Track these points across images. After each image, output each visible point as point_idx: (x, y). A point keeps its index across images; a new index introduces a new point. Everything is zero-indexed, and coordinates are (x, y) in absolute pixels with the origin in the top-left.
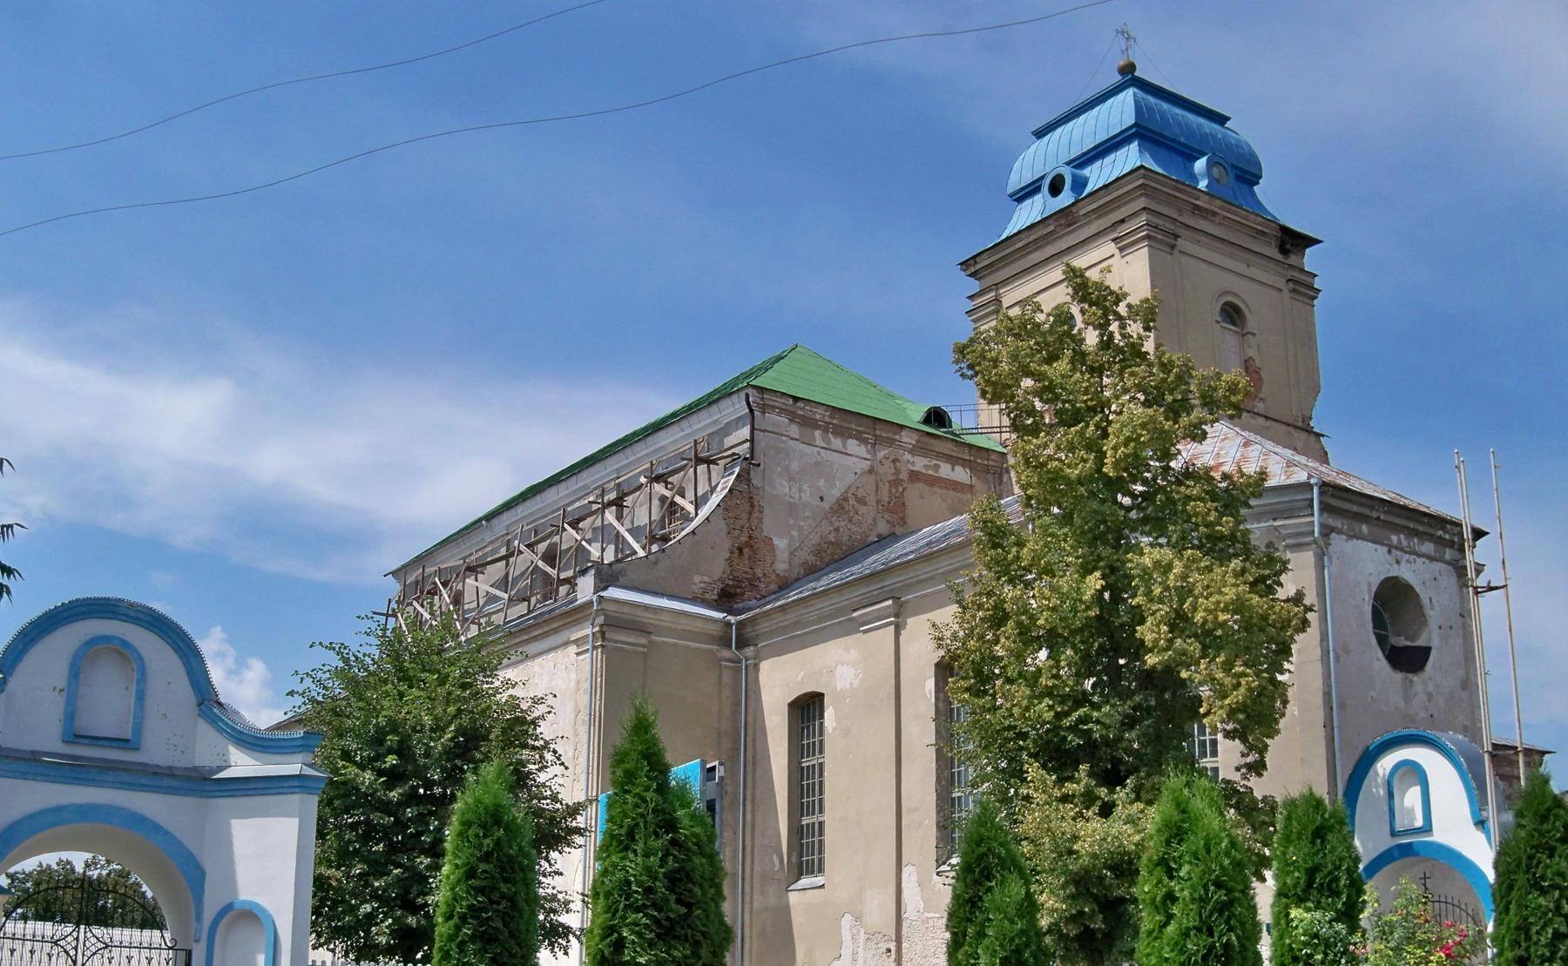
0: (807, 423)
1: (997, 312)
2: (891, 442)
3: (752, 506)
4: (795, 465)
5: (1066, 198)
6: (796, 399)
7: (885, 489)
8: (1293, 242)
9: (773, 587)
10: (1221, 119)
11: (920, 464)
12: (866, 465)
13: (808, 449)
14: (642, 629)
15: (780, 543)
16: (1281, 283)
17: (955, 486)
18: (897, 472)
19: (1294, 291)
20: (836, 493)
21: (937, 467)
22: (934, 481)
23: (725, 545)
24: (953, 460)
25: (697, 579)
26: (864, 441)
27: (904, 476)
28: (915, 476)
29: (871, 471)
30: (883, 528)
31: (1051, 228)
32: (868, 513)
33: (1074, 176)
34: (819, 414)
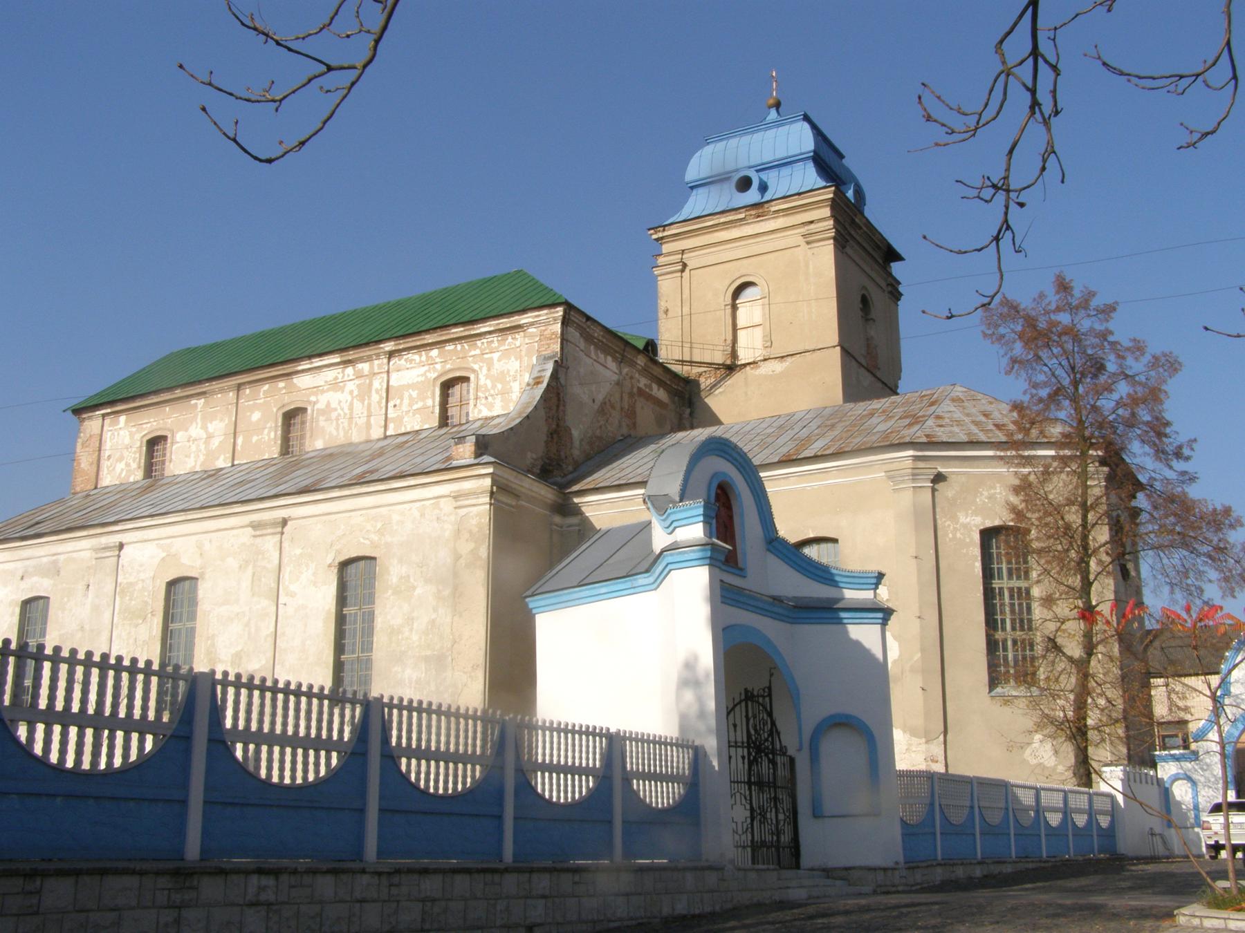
0: (588, 338)
1: (682, 271)
2: (633, 364)
3: (559, 400)
4: (582, 370)
5: (752, 196)
6: (588, 318)
7: (626, 397)
8: (892, 255)
9: (570, 468)
10: (841, 156)
11: (643, 382)
12: (615, 378)
13: (589, 361)
14: (517, 496)
15: (575, 433)
16: (883, 284)
17: (658, 402)
18: (632, 387)
19: (890, 293)
20: (600, 398)
21: (651, 389)
22: (649, 397)
23: (545, 429)
24: (661, 383)
25: (529, 455)
26: (615, 359)
27: (635, 390)
28: (641, 392)
29: (618, 383)
30: (625, 431)
31: (742, 216)
32: (616, 414)
33: (761, 180)
34: (598, 333)
